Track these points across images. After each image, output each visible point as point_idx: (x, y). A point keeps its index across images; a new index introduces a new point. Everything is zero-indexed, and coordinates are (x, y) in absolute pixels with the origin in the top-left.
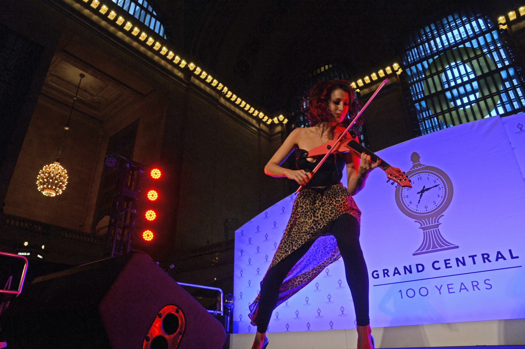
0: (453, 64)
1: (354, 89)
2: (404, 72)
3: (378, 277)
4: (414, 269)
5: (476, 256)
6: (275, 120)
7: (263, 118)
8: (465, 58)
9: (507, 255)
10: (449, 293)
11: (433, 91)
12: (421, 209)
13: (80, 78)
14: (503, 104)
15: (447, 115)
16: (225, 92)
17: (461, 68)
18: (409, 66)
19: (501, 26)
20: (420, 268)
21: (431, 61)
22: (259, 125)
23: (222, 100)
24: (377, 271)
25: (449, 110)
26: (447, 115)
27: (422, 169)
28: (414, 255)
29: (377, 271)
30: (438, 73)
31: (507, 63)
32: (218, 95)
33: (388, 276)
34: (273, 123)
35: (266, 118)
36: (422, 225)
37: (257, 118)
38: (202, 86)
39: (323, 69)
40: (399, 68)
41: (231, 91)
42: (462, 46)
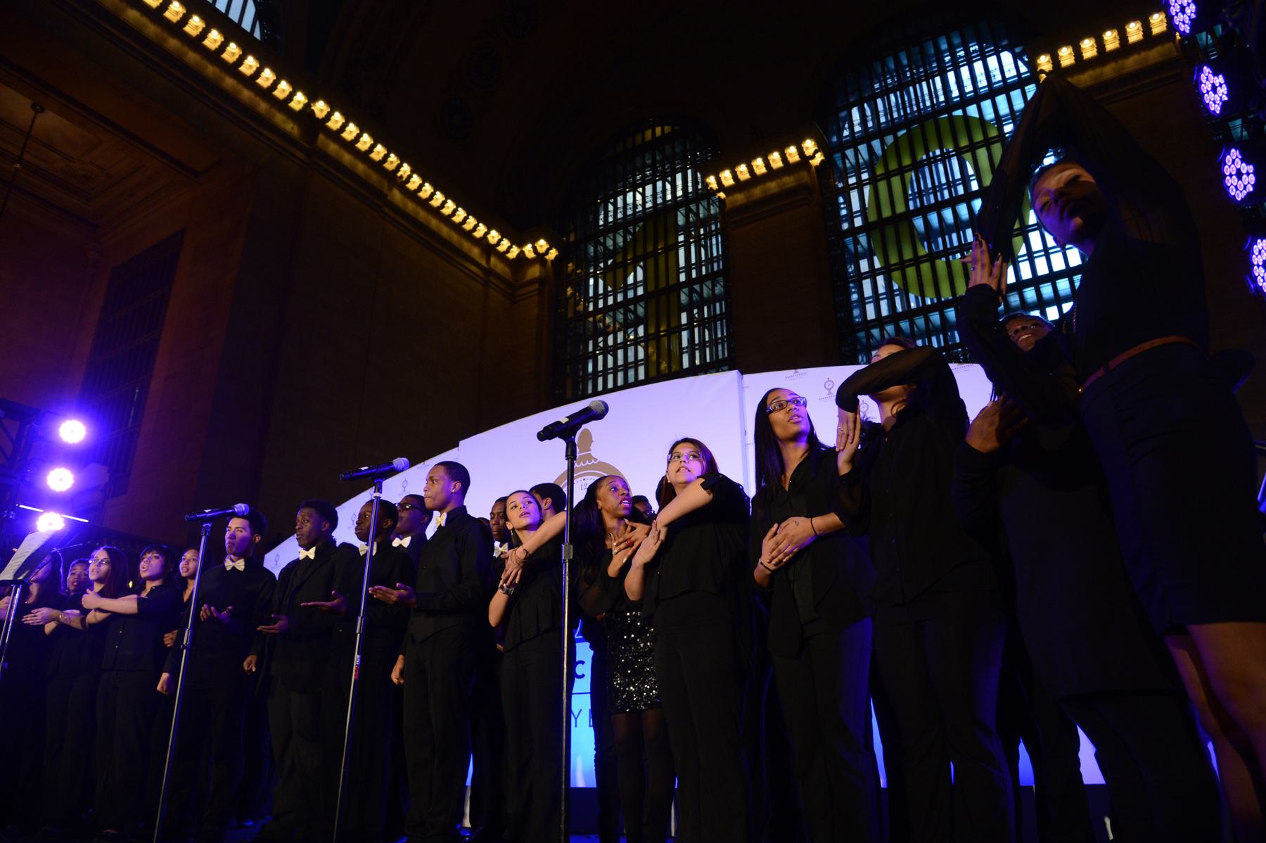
1: (714, 193)
6: (528, 249)
8: (964, 142)
11: (886, 213)
13: (33, 113)
15: (911, 271)
21: (889, 139)
22: (488, 261)
23: (397, 196)
25: (917, 261)
32: (385, 185)
34: (522, 254)
35: (505, 244)
38: (347, 158)
39: (649, 134)
40: (816, 152)
42: (959, 113)
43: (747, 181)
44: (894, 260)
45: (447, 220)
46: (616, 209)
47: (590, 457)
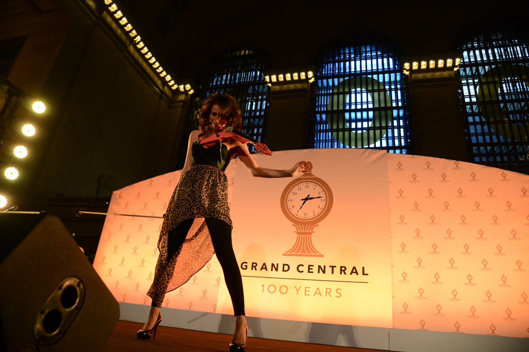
0: (359, 89)
1: (266, 83)
2: (315, 82)
3: (246, 269)
4: (280, 268)
5: (335, 267)
6: (182, 87)
7: (170, 81)
8: (370, 88)
9: (360, 271)
10: (305, 294)
11: (335, 108)
12: (301, 215)
14: (387, 138)
15: (341, 134)
16: (137, 41)
17: (364, 95)
18: (322, 78)
19: (405, 71)
20: (286, 268)
21: (341, 80)
22: (163, 88)
23: (131, 49)
24: (246, 263)
25: (344, 130)
26: (341, 134)
27: (312, 179)
28: (284, 255)
29: (246, 263)
30: (344, 93)
31: (400, 104)
33: (256, 269)
35: (172, 82)
36: (297, 230)
37: (163, 79)
40: (312, 77)
41: (144, 43)
42: (370, 76)
43: (282, 82)
44: (335, 127)
45: (151, 65)
46: (217, 81)
47: (311, 175)
